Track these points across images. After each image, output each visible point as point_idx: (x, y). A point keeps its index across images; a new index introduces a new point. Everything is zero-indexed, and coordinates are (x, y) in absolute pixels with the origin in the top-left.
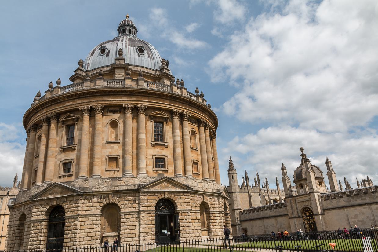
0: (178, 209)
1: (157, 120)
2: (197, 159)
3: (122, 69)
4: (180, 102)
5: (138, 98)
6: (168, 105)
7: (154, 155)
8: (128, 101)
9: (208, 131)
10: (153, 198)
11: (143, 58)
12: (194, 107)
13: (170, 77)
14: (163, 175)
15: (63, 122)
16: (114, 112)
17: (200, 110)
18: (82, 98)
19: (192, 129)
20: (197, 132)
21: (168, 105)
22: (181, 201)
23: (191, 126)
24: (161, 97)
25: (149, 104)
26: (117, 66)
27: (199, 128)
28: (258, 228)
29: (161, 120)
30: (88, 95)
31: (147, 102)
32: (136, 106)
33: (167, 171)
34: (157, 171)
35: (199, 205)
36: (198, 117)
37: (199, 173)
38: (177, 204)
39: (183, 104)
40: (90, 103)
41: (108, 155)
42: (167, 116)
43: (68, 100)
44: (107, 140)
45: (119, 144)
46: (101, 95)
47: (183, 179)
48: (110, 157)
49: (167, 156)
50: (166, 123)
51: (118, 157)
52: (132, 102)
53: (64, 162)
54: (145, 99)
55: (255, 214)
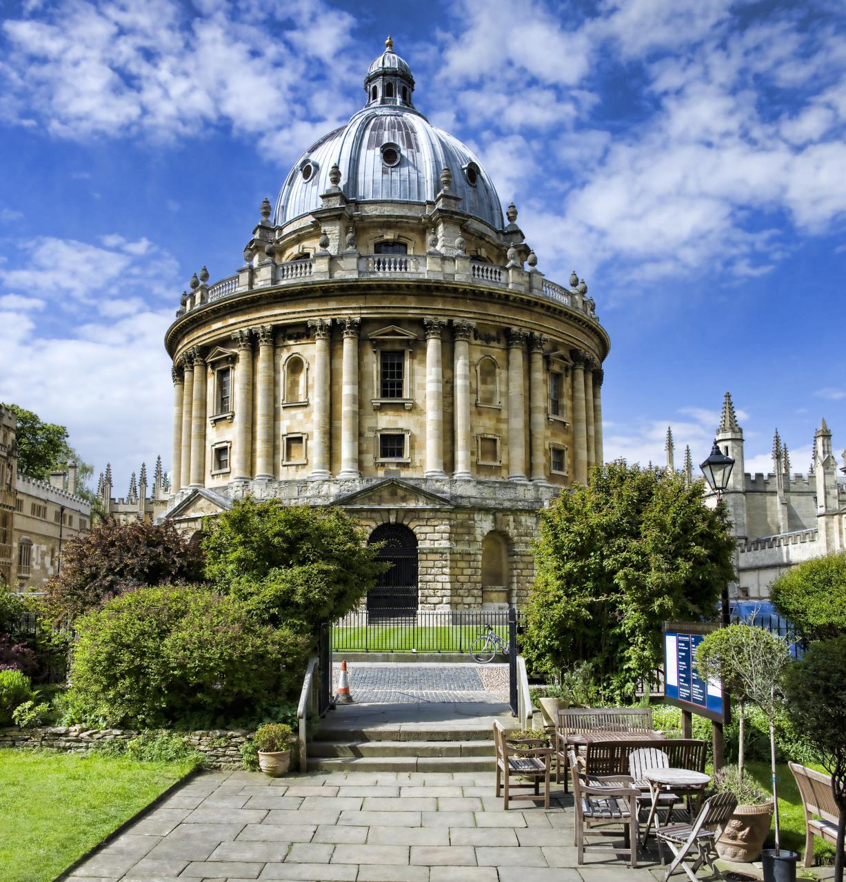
0: (420, 546)
1: (388, 347)
3: (334, 220)
4: (447, 297)
5: (342, 301)
6: (412, 308)
8: (319, 310)
11: (395, 176)
12: (490, 302)
13: (456, 217)
14: (398, 472)
15: (214, 365)
16: (298, 337)
17: (513, 306)
18: (236, 311)
20: (501, 362)
21: (412, 308)
23: (482, 352)
24: (395, 292)
25: (367, 314)
26: (323, 215)
27: (507, 350)
28: (549, 592)
29: (398, 347)
30: (246, 306)
31: (361, 308)
32: (334, 321)
34: (383, 465)
35: (480, 538)
36: (503, 325)
38: (418, 536)
39: (456, 300)
40: (250, 323)
41: (285, 433)
42: (411, 334)
43: (216, 318)
44: (285, 402)
45: (305, 410)
46: (268, 304)
48: (290, 436)
49: (408, 431)
50: (410, 352)
51: (305, 437)
52: (328, 313)
53: (217, 446)
54: (357, 301)
55: (765, 553)
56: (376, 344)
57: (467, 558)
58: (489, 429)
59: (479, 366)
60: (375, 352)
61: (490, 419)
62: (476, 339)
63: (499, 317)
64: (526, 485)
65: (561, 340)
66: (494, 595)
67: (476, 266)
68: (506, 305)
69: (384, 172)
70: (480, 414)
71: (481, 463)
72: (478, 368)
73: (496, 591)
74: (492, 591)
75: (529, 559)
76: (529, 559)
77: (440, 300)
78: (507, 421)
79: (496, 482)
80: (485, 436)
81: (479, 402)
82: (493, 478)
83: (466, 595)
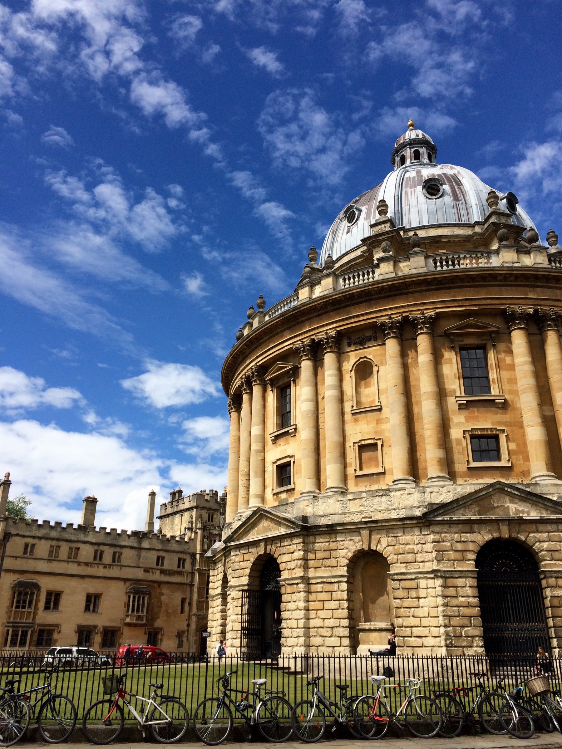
1: (281, 383)
2: (376, 432)
7: (274, 463)
9: (423, 341)
10: (246, 557)
11: (354, 229)
12: (352, 305)
19: (361, 360)
22: (286, 558)
23: (356, 356)
25: (261, 361)
31: (258, 357)
33: (294, 489)
34: (277, 494)
37: (381, 470)
47: (306, 503)
49: (292, 457)
56: (273, 382)
57: (328, 587)
58: (368, 434)
59: (353, 371)
60: (272, 390)
61: (368, 423)
62: (349, 346)
63: (363, 315)
64: (404, 489)
65: (463, 309)
66: (375, 634)
67: (347, 277)
68: (371, 300)
69: (348, 232)
70: (356, 421)
71: (359, 473)
72: (353, 373)
73: (375, 630)
74: (370, 630)
75: (413, 584)
76: (413, 584)
77: (307, 324)
78: (387, 419)
79: (363, 492)
80: (363, 443)
81: (355, 408)
82: (375, 487)
83: (329, 634)
